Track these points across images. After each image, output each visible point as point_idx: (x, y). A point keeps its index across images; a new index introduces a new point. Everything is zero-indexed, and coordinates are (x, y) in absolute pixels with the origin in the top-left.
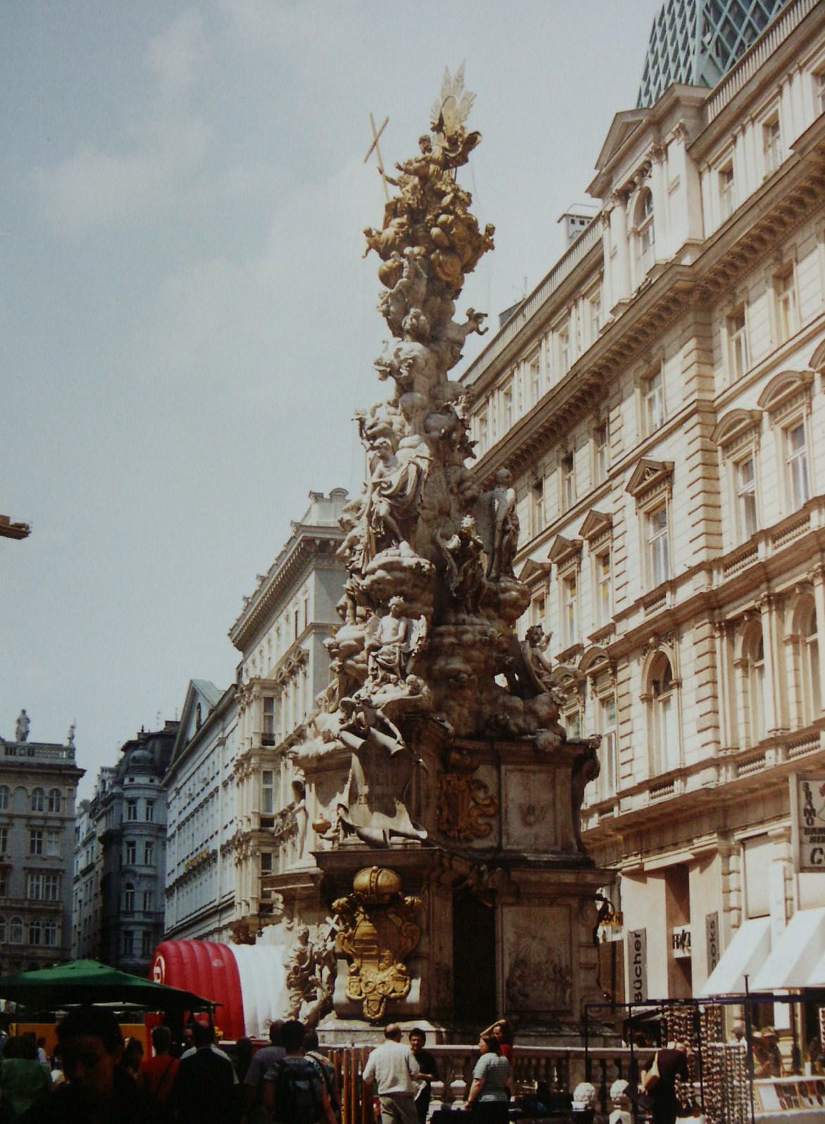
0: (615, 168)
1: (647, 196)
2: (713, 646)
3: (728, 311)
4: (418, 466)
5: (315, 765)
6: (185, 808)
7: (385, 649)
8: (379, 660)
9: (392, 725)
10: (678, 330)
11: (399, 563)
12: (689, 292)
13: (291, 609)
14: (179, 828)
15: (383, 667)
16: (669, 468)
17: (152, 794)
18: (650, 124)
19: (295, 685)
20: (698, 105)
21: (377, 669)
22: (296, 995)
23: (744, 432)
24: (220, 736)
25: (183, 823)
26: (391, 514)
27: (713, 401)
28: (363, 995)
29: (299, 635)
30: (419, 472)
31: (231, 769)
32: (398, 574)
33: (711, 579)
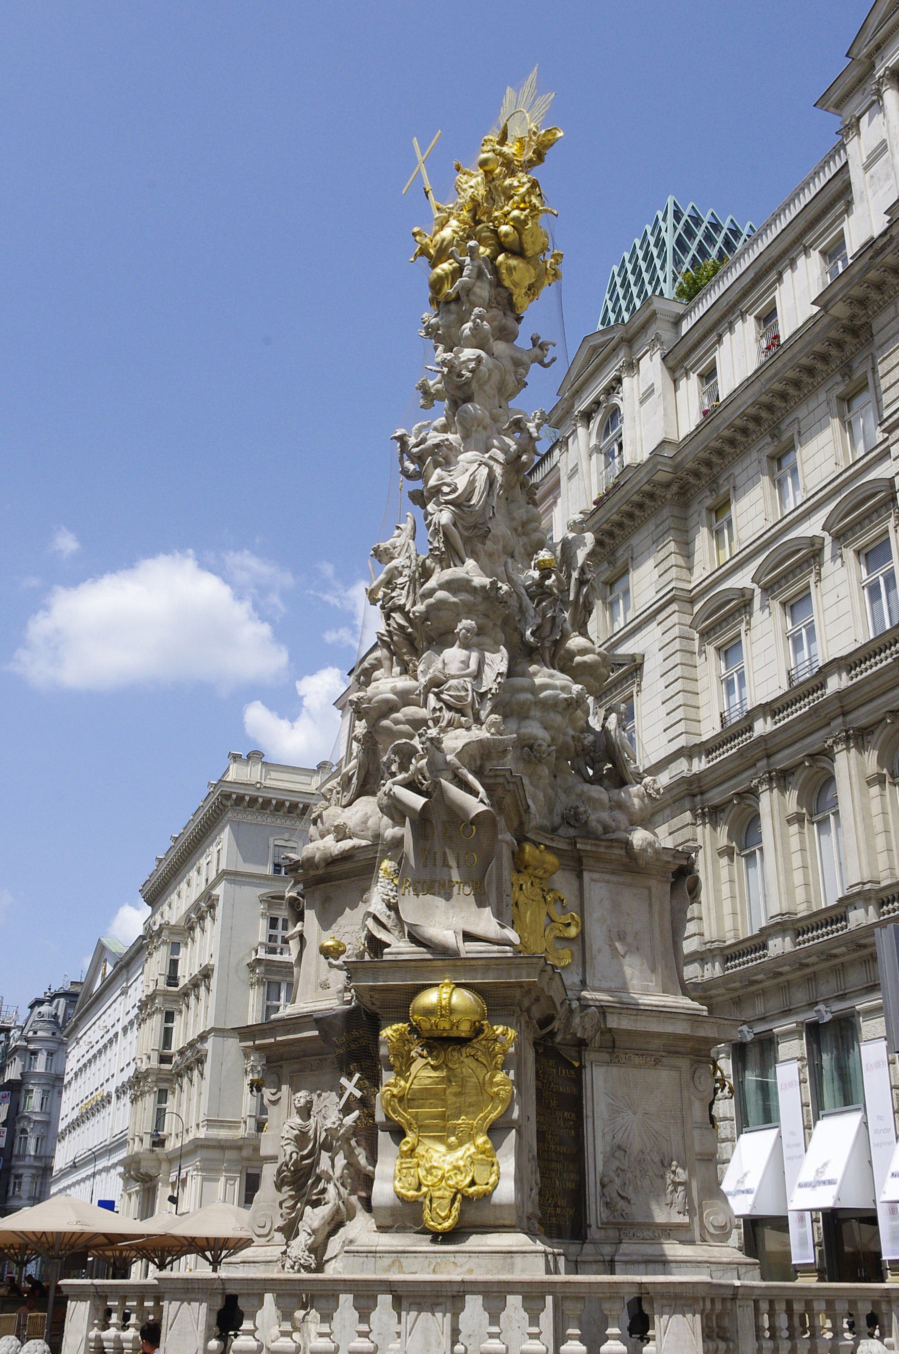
0: (578, 393)
1: (614, 414)
2: (695, 833)
3: (709, 502)
4: (490, 468)
5: (321, 872)
6: (83, 1056)
7: (452, 682)
8: (444, 696)
9: (471, 778)
10: (651, 526)
11: (469, 581)
12: (667, 485)
13: (203, 862)
14: (76, 1074)
15: (450, 708)
16: (638, 661)
17: (51, 1046)
18: (622, 340)
19: (203, 930)
20: (673, 320)
21: (441, 709)
22: (291, 1197)
23: (732, 614)
24: (124, 985)
25: (80, 1070)
26: (455, 525)
27: (691, 591)
28: (424, 1189)
29: (209, 882)
30: (491, 480)
31: (136, 1011)
32: (464, 596)
33: (691, 765)
